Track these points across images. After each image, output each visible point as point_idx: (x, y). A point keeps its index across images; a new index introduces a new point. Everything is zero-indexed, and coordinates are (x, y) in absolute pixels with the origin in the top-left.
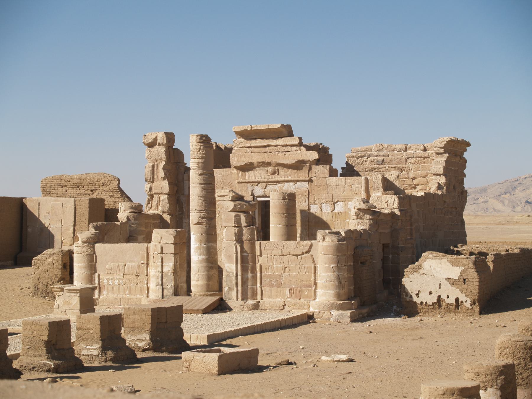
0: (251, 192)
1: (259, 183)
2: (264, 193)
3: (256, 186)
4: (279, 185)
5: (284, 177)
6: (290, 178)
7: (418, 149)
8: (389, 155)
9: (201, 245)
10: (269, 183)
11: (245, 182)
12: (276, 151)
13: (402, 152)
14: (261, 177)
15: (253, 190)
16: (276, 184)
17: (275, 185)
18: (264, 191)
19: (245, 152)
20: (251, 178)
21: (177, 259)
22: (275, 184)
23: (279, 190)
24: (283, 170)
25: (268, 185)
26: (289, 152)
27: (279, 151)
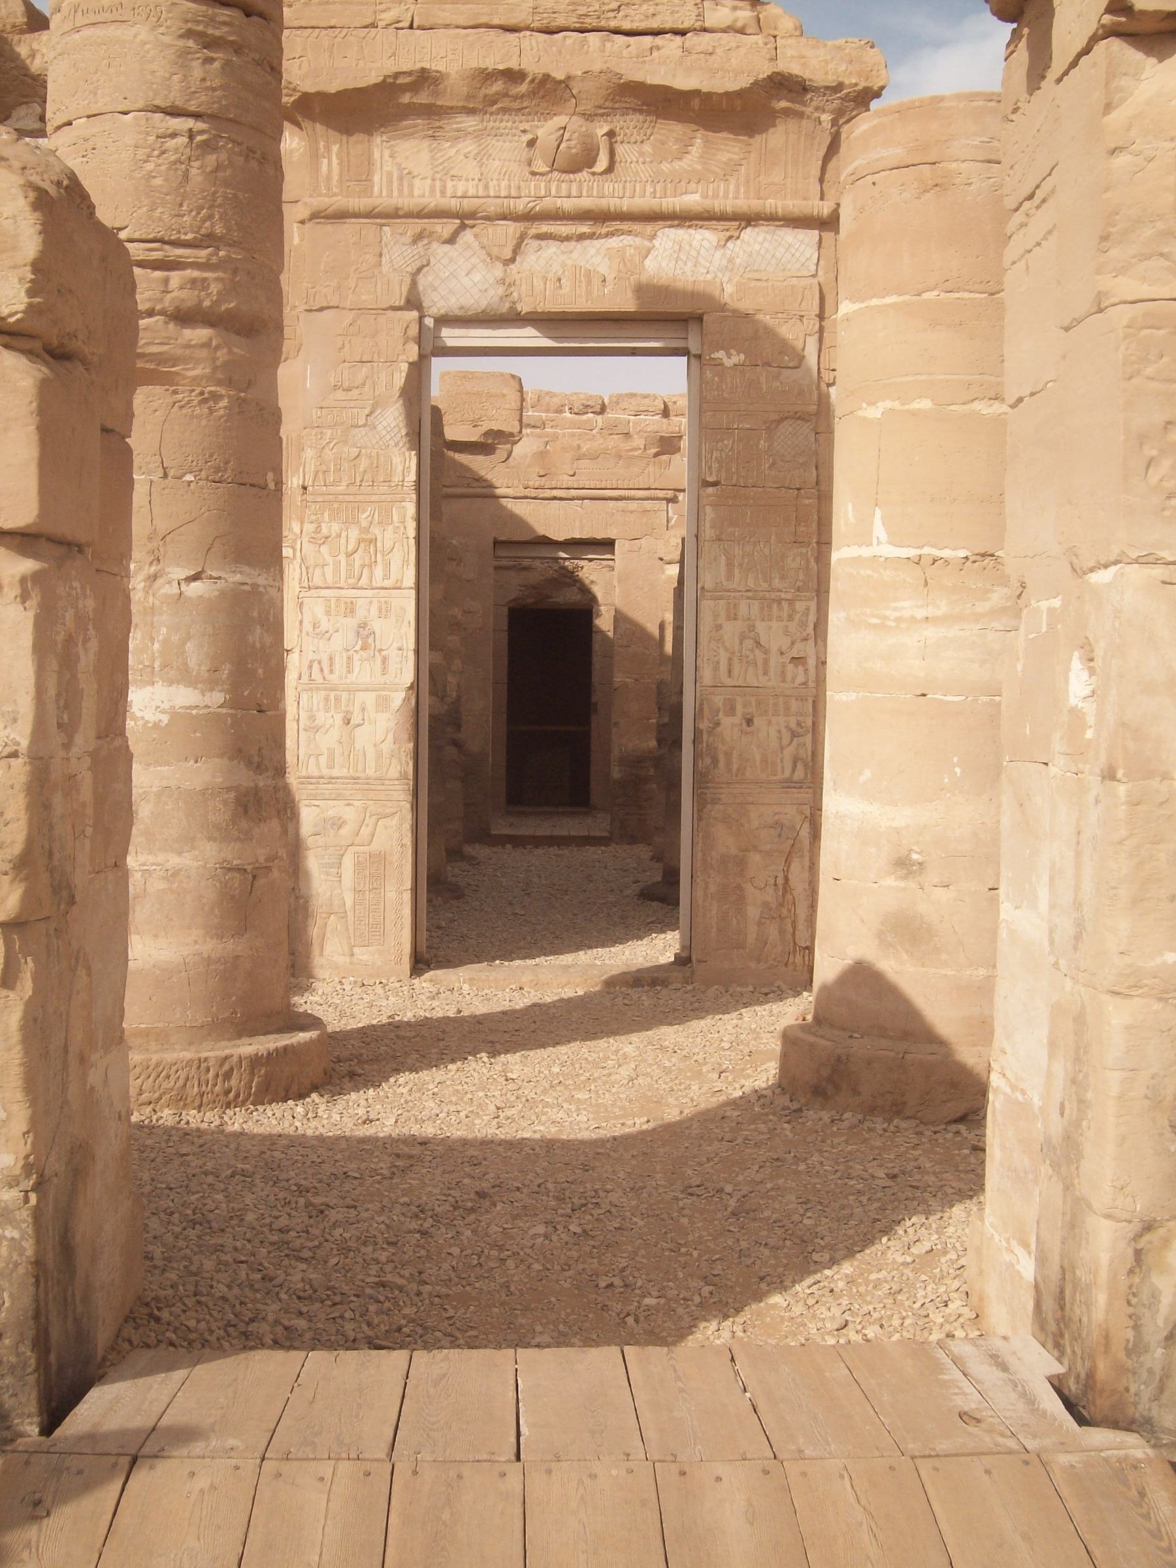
0: (408, 280)
1: (466, 218)
2: (501, 291)
3: (447, 247)
4: (614, 242)
5: (649, 189)
6: (692, 200)
7: (645, 408)
8: (544, 424)
9: (155, 577)
10: (545, 228)
11: (369, 215)
12: (590, 22)
13: (591, 415)
14: (486, 187)
15: (419, 270)
16: (591, 236)
17: (587, 242)
18: (502, 281)
19: (369, 21)
20: (411, 186)
21: (68, 661)
22: (581, 237)
23: (610, 278)
24: (647, 148)
25: (535, 243)
26: (682, 33)
27: (613, 24)
